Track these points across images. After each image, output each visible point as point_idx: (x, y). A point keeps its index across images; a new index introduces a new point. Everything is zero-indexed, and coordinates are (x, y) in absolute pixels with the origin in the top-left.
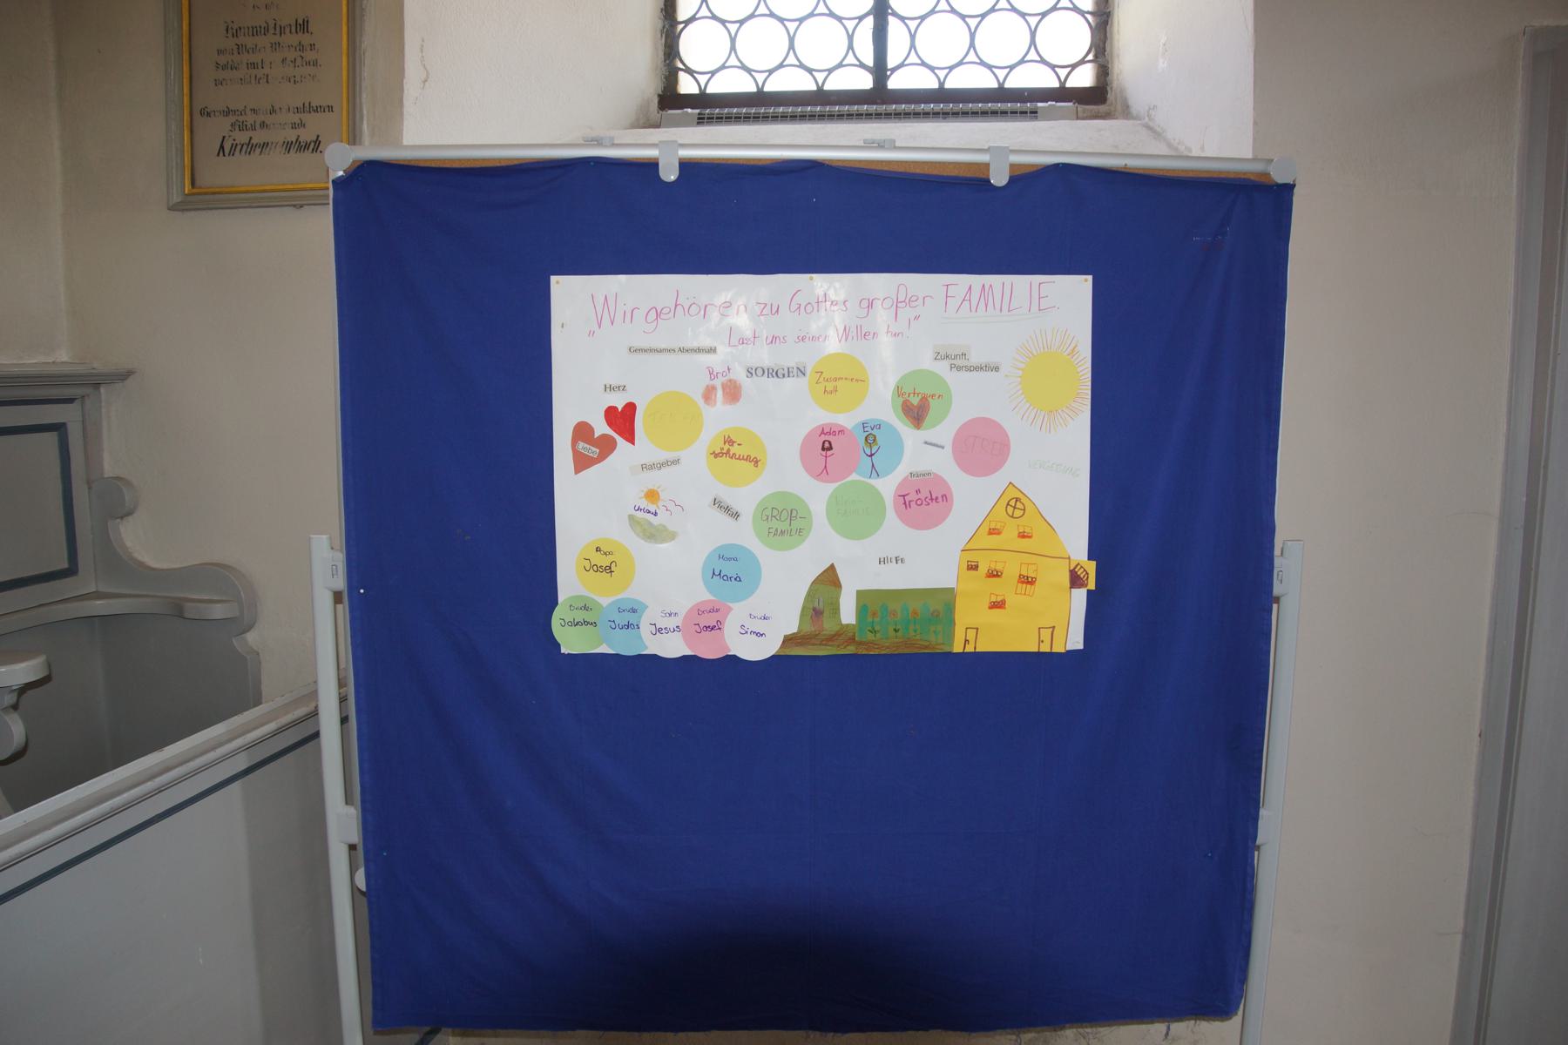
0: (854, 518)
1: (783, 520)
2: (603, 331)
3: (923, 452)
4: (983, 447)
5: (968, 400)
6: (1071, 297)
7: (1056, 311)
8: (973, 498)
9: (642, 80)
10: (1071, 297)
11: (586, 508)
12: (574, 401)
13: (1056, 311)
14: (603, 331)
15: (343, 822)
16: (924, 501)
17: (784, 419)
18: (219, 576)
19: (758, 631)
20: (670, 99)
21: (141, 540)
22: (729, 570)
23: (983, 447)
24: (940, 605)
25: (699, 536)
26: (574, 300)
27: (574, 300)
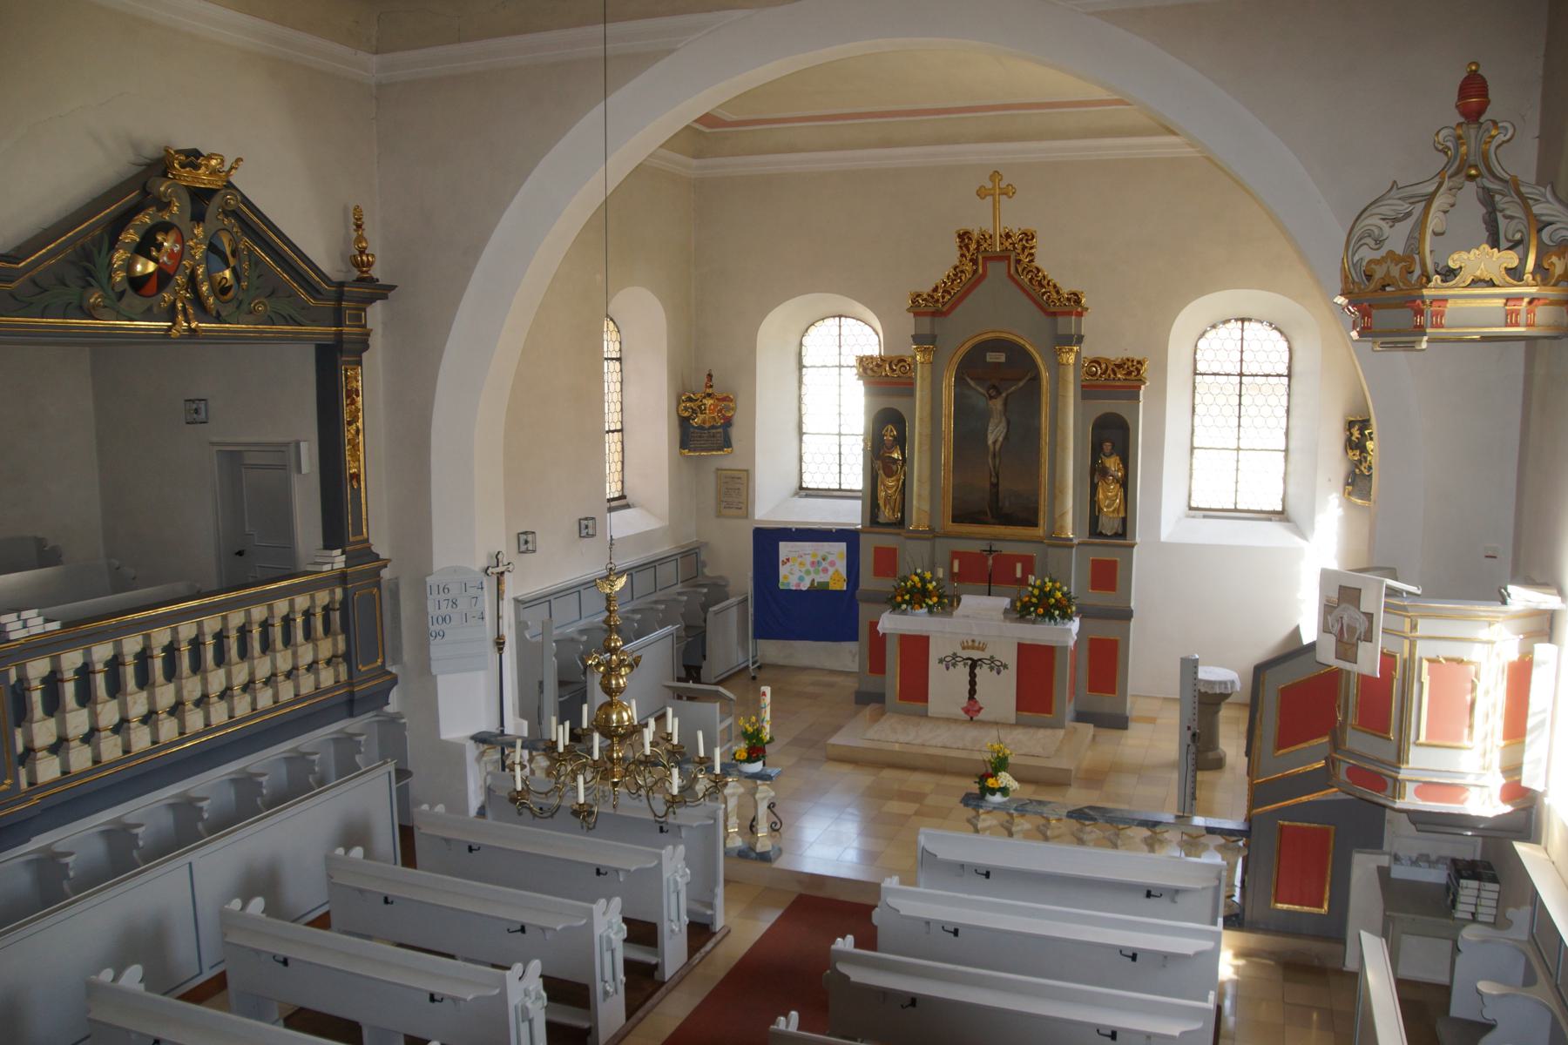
0: (817, 572)
1: (808, 572)
2: (785, 549)
3: (825, 564)
4: (832, 564)
5: (830, 558)
6: (844, 545)
7: (841, 547)
8: (831, 570)
9: (795, 485)
10: (844, 545)
11: (783, 570)
12: (782, 557)
13: (841, 547)
14: (785, 549)
15: (751, 610)
16: (825, 570)
17: (809, 560)
18: (721, 577)
19: (805, 586)
20: (801, 488)
21: (707, 571)
22: (801, 579)
23: (832, 564)
24: (827, 584)
25: (798, 574)
26: (782, 545)
27: (782, 545)
